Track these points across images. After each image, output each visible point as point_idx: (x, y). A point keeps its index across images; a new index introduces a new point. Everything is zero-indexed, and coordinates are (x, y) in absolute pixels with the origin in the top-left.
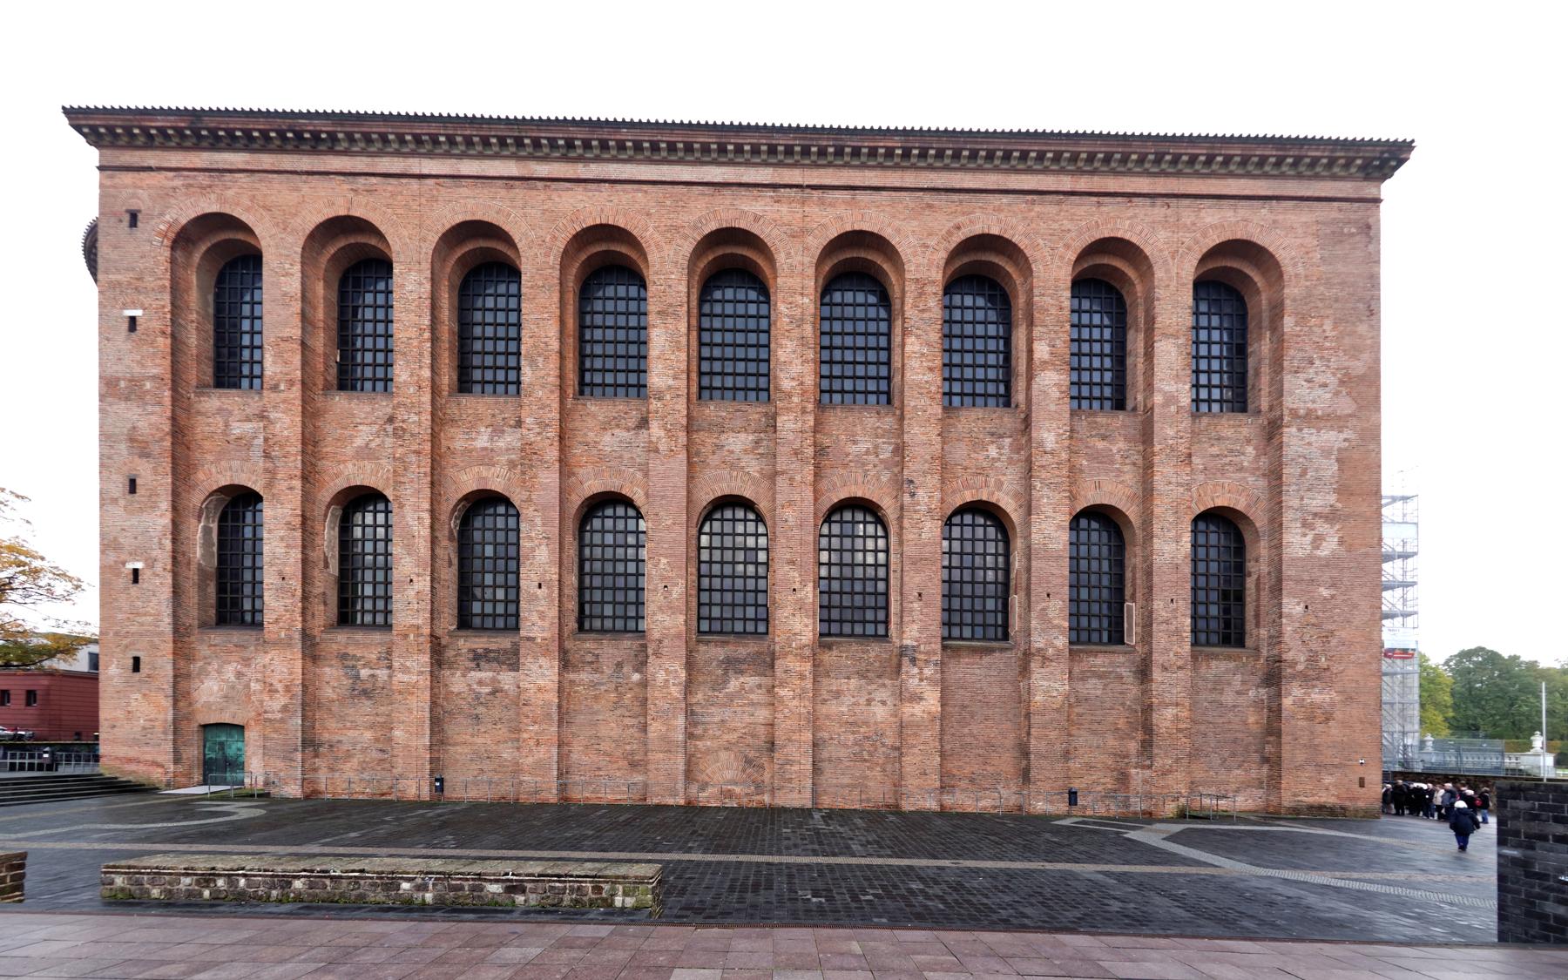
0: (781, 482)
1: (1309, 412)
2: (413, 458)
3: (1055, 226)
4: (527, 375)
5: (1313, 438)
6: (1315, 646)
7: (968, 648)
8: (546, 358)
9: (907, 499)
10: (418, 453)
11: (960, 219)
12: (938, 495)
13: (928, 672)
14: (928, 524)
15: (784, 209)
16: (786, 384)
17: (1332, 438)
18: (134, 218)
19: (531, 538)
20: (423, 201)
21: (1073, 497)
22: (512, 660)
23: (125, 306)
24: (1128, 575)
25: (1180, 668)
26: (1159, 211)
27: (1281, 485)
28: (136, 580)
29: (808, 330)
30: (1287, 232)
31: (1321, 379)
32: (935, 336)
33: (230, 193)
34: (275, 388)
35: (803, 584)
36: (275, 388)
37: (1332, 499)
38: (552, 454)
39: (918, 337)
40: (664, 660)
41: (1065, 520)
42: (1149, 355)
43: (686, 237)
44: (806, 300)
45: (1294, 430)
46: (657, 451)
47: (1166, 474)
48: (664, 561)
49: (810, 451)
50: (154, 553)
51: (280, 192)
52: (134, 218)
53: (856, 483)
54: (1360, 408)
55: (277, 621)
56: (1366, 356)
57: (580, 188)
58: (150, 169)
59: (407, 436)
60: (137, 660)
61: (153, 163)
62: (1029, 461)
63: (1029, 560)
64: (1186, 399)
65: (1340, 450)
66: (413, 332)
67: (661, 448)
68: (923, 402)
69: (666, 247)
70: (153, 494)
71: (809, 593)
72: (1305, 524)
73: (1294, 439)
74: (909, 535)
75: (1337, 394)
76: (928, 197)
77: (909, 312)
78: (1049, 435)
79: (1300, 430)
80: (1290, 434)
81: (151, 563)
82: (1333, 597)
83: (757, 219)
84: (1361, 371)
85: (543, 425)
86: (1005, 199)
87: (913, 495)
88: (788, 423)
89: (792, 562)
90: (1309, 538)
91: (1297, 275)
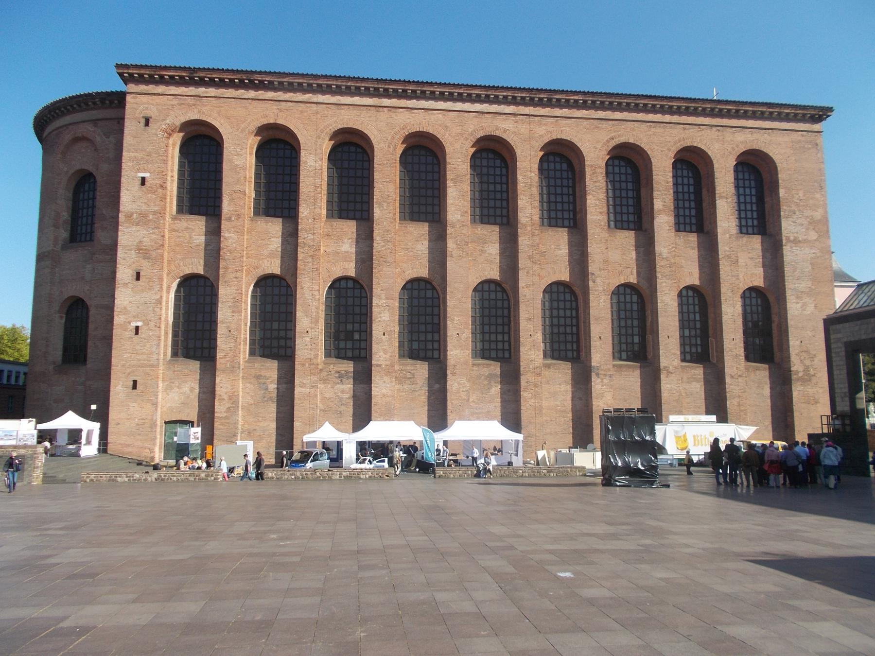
1: (795, 238)
2: (310, 260)
3: (662, 139)
5: (798, 252)
6: (807, 363)
7: (627, 365)
10: (312, 257)
11: (613, 134)
13: (606, 381)
14: (603, 298)
15: (520, 126)
18: (147, 122)
19: (378, 306)
20: (319, 116)
23: (138, 171)
25: (740, 376)
26: (714, 133)
29: (535, 191)
31: (799, 221)
33: (205, 109)
34: (229, 219)
36: (229, 219)
37: (809, 284)
39: (593, 195)
41: (674, 294)
43: (467, 139)
44: (533, 175)
45: (788, 247)
46: (452, 256)
48: (457, 319)
51: (236, 109)
52: (147, 122)
56: (820, 211)
57: (407, 112)
58: (159, 94)
59: (307, 247)
65: (812, 258)
66: (311, 188)
68: (598, 230)
70: (150, 280)
72: (798, 298)
73: (790, 253)
75: (807, 229)
76: (596, 122)
79: (791, 247)
82: (814, 336)
83: (505, 131)
84: (819, 218)
86: (637, 125)
87: (594, 281)
90: (799, 305)
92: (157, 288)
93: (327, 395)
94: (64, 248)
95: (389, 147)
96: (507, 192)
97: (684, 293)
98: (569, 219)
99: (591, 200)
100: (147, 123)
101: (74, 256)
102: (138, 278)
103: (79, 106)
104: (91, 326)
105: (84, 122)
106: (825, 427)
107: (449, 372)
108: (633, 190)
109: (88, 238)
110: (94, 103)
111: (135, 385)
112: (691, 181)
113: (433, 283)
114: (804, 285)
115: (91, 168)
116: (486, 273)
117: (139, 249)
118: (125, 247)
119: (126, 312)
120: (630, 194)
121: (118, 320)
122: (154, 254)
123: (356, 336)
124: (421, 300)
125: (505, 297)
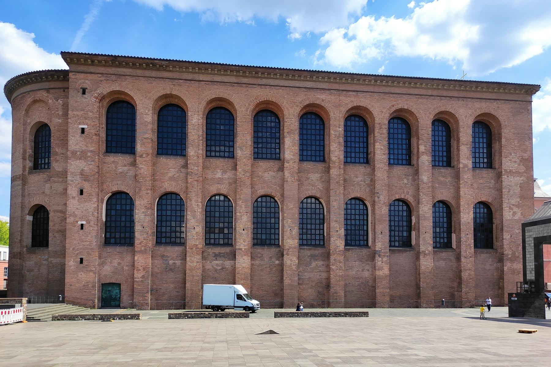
0: (332, 193)
1: (511, 171)
4: (239, 153)
8: (246, 147)
9: (376, 199)
12: (387, 197)
16: (333, 158)
17: (519, 180)
19: (240, 212)
21: (433, 198)
22: (233, 256)
24: (453, 224)
27: (502, 195)
28: (82, 228)
29: (342, 140)
30: (502, 111)
32: (386, 143)
35: (340, 229)
38: (248, 182)
39: (380, 143)
40: (290, 256)
41: (430, 206)
42: (458, 150)
43: (297, 106)
44: (340, 129)
46: (287, 181)
47: (463, 191)
48: (290, 220)
49: (342, 182)
50: (90, 218)
53: (357, 192)
54: (527, 169)
55: (140, 244)
60: (82, 260)
62: (418, 185)
63: (419, 220)
64: (470, 165)
67: (289, 180)
69: (290, 109)
71: (342, 232)
72: (510, 208)
73: (507, 180)
74: (377, 212)
75: (519, 165)
77: (376, 134)
78: (425, 176)
79: (508, 177)
80: (504, 177)
81: (88, 222)
85: (245, 171)
87: (379, 197)
88: (334, 172)
89: (337, 221)
91: (505, 125)
92: (95, 200)
93: (207, 267)
94: (30, 173)
95: (247, 111)
96: (324, 140)
97: (437, 205)
98: (364, 158)
99: (378, 146)
100: (84, 93)
101: (36, 179)
103: (36, 79)
104: (51, 224)
106: (519, 289)
107: (285, 253)
108: (406, 139)
109: (46, 167)
110: (47, 78)
111: (82, 261)
112: (444, 134)
113: (276, 198)
114: (513, 201)
115: (46, 121)
116: (310, 192)
118: (72, 173)
120: (404, 142)
122: (92, 178)
123: (226, 231)
124: (268, 209)
125: (321, 207)
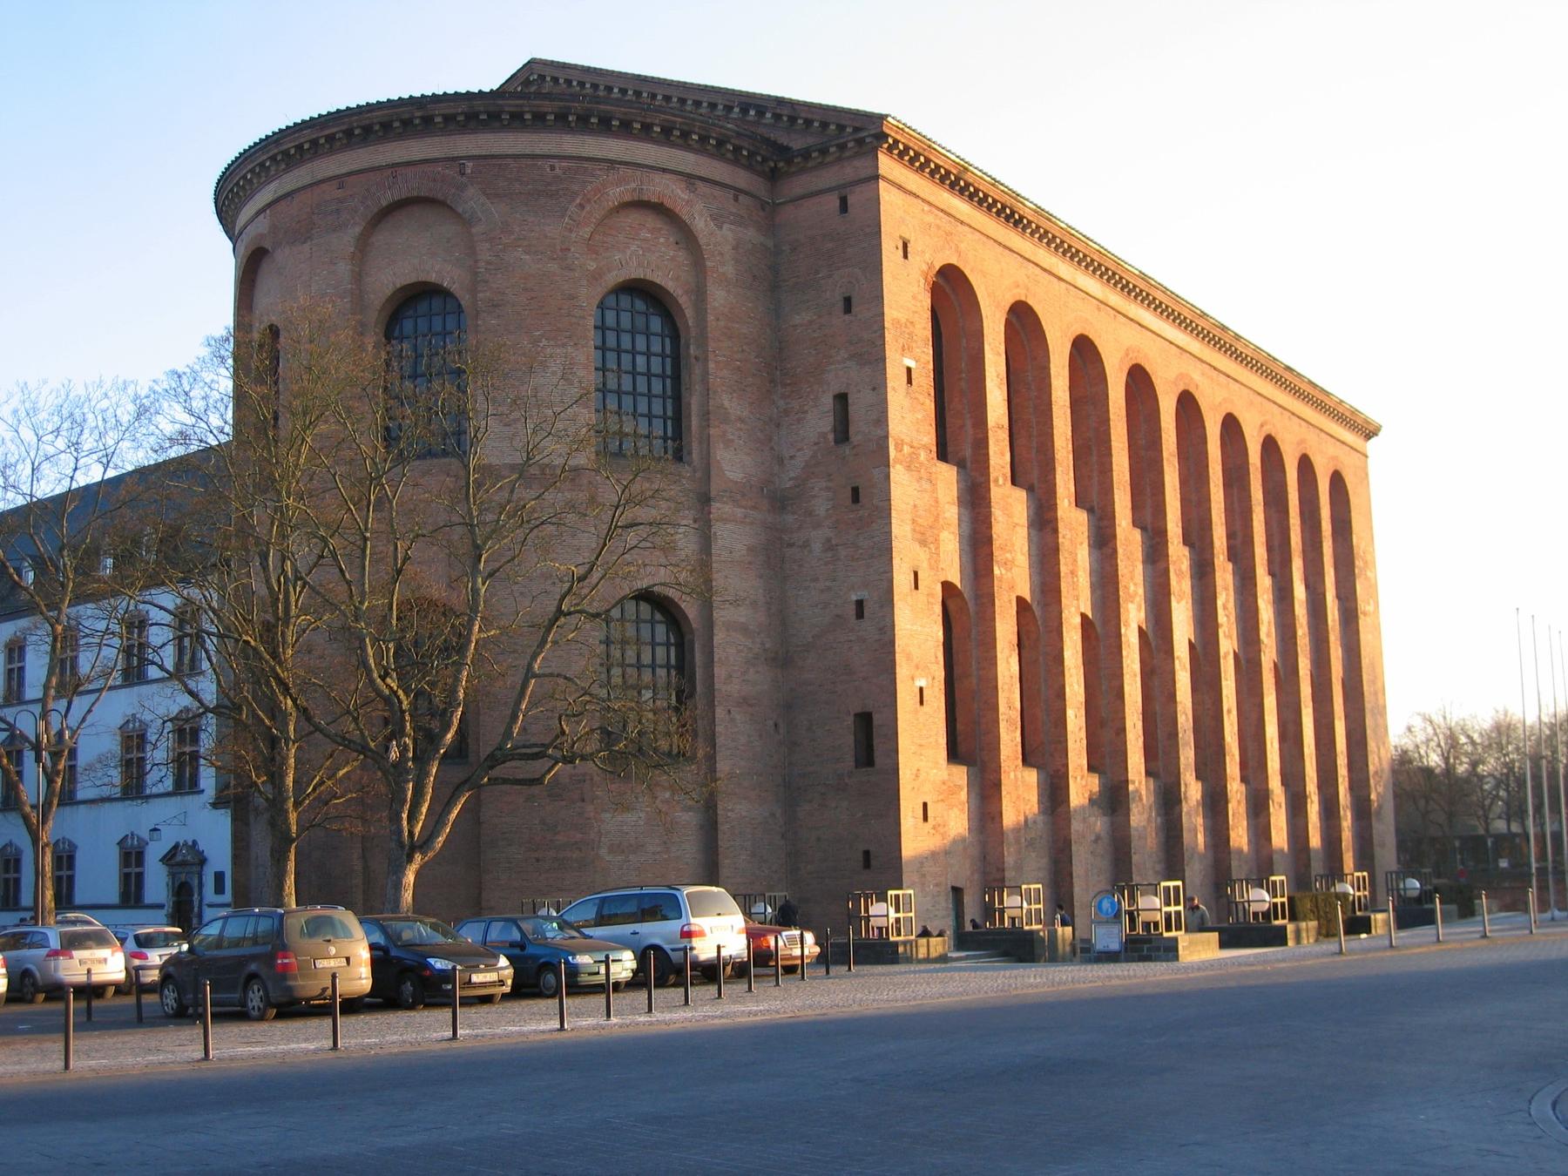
36: (996, 480)
61: (912, 187)
102: (916, 587)
105: (664, 170)
117: (914, 521)
119: (909, 657)
121: (902, 671)
